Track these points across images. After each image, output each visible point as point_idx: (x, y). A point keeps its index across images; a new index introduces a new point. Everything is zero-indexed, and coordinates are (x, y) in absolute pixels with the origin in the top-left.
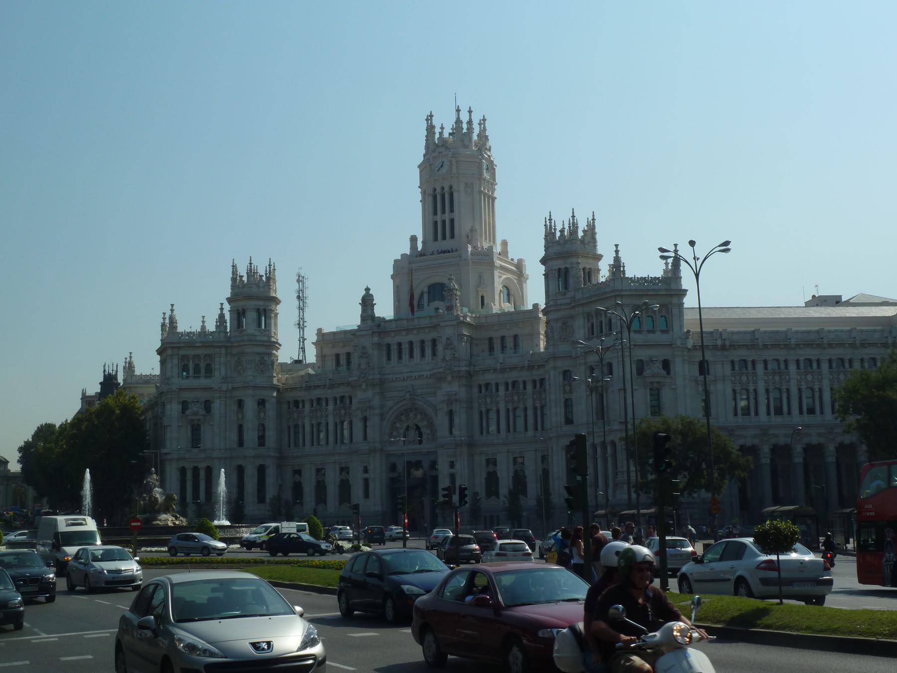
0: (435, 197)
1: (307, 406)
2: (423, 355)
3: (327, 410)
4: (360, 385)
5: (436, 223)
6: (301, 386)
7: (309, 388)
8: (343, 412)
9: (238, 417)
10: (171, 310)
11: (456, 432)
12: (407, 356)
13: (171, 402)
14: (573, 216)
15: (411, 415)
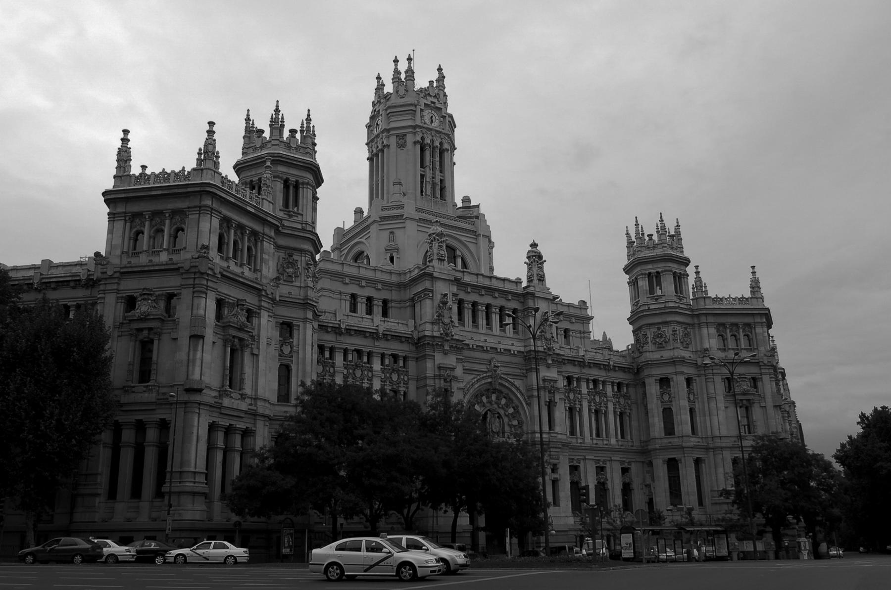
0: (422, 150)
1: (339, 359)
2: (502, 326)
3: (371, 370)
4: (442, 346)
5: (422, 176)
6: (337, 326)
7: (349, 332)
8: (395, 377)
9: (282, 350)
10: (208, 132)
11: (558, 429)
12: (485, 322)
13: (206, 294)
14: (678, 226)
15: (494, 397)
